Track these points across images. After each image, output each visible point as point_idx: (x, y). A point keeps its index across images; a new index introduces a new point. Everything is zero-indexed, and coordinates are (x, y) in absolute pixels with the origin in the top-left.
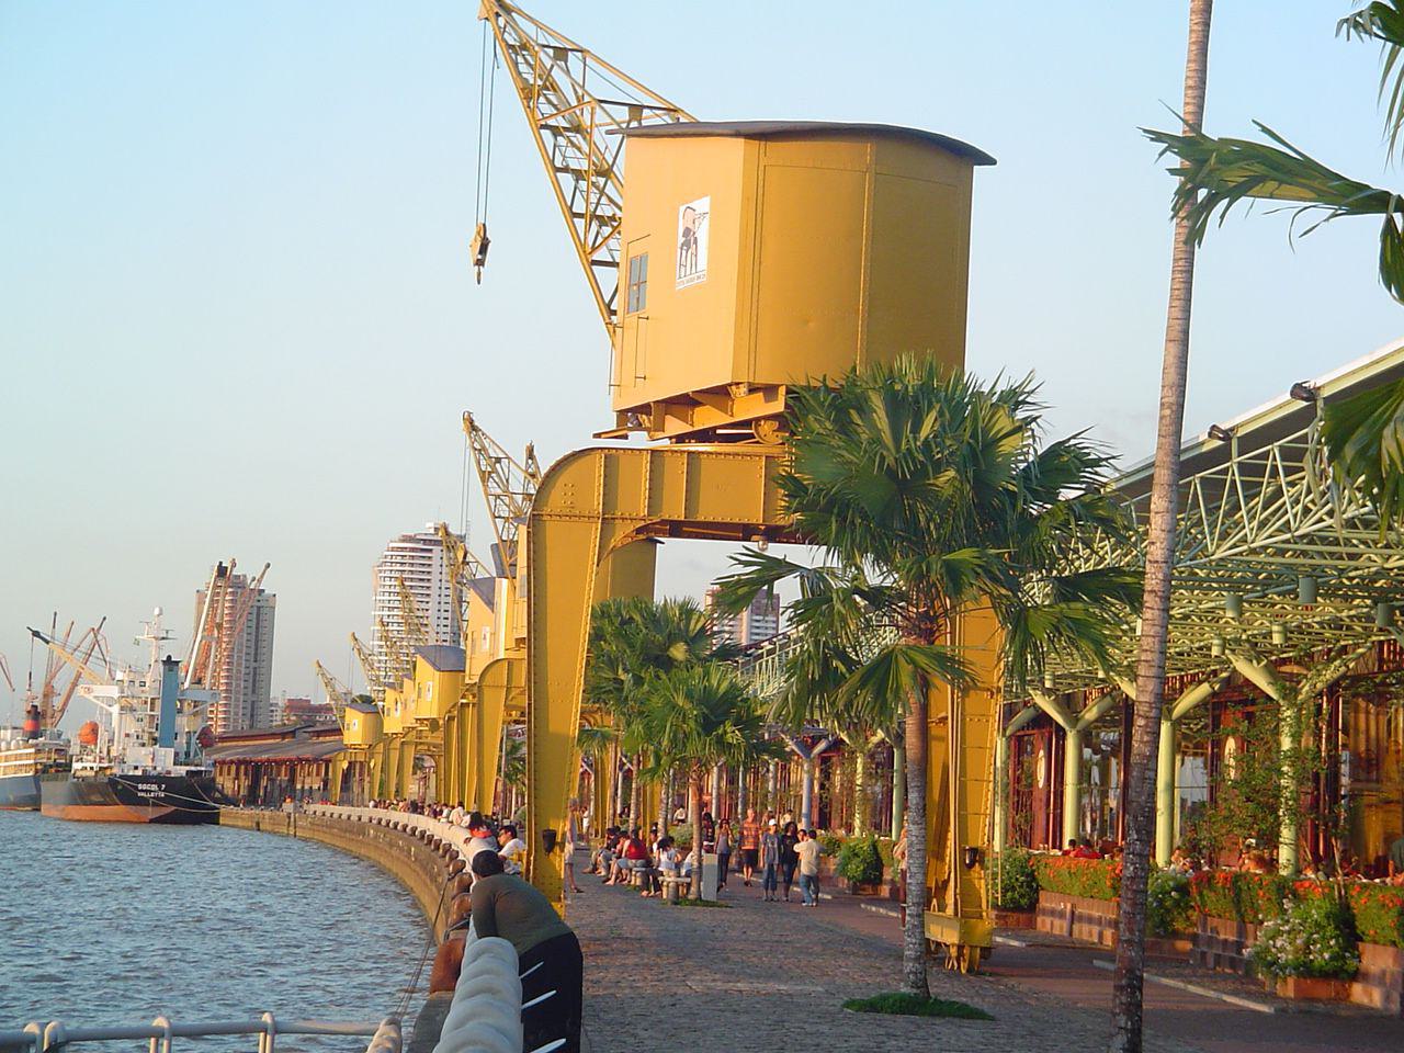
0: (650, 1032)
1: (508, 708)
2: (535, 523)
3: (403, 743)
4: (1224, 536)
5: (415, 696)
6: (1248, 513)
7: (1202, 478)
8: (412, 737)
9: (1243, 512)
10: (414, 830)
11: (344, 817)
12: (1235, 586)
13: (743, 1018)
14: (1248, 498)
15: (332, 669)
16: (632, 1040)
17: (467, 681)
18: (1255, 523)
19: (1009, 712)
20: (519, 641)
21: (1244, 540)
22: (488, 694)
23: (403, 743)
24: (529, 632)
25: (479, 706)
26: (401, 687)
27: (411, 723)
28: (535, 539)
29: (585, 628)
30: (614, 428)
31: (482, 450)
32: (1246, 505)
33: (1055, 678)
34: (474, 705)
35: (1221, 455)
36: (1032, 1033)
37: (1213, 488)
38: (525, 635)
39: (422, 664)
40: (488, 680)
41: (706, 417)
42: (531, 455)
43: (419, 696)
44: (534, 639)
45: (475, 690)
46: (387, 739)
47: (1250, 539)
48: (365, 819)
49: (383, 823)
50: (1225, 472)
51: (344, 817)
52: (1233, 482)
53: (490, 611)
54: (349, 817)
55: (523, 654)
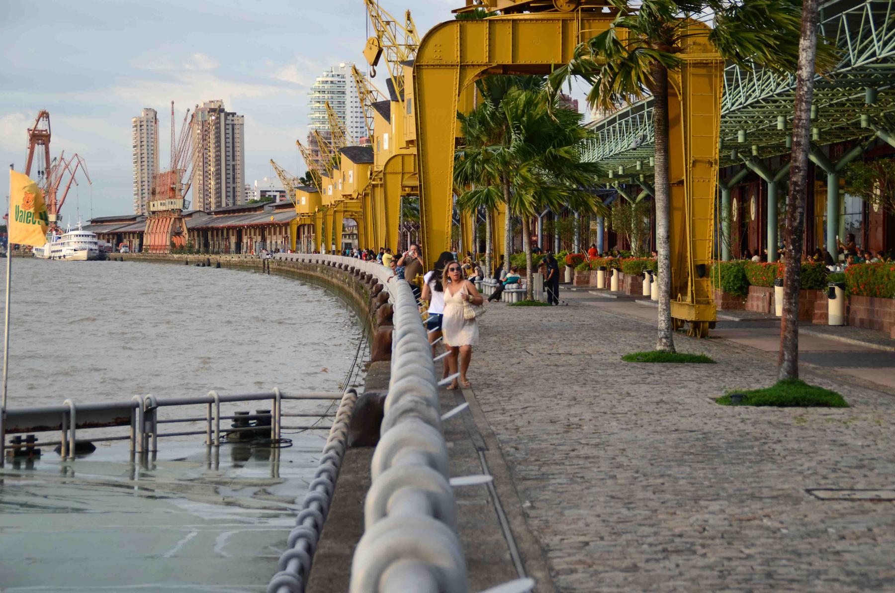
0: (506, 378)
1: (403, 187)
2: (417, 67)
3: (335, 212)
4: (861, 52)
5: (340, 181)
6: (877, 36)
7: (847, 15)
8: (341, 207)
9: (874, 36)
10: (346, 267)
11: (300, 260)
12: (873, 84)
13: (561, 369)
14: (878, 24)
15: (282, 165)
16: (495, 383)
17: (375, 169)
18: (881, 43)
19: (724, 175)
20: (411, 142)
21: (874, 54)
22: (389, 178)
23: (335, 212)
24: (417, 135)
25: (384, 186)
26: (332, 175)
27: (339, 197)
28: (417, 79)
29: (454, 129)
30: (464, 6)
31: (376, 17)
32: (876, 30)
33: (759, 149)
34: (381, 185)
36: (738, 369)
37: (854, 21)
38: (414, 137)
39: (344, 159)
40: (389, 170)
42: (409, 19)
43: (344, 180)
44: (420, 141)
45: (381, 175)
46: (323, 209)
47: (878, 52)
48: (314, 261)
49: (326, 263)
50: (862, 9)
51: (300, 260)
52: (867, 15)
53: (386, 122)
54: (303, 260)
55: (413, 150)
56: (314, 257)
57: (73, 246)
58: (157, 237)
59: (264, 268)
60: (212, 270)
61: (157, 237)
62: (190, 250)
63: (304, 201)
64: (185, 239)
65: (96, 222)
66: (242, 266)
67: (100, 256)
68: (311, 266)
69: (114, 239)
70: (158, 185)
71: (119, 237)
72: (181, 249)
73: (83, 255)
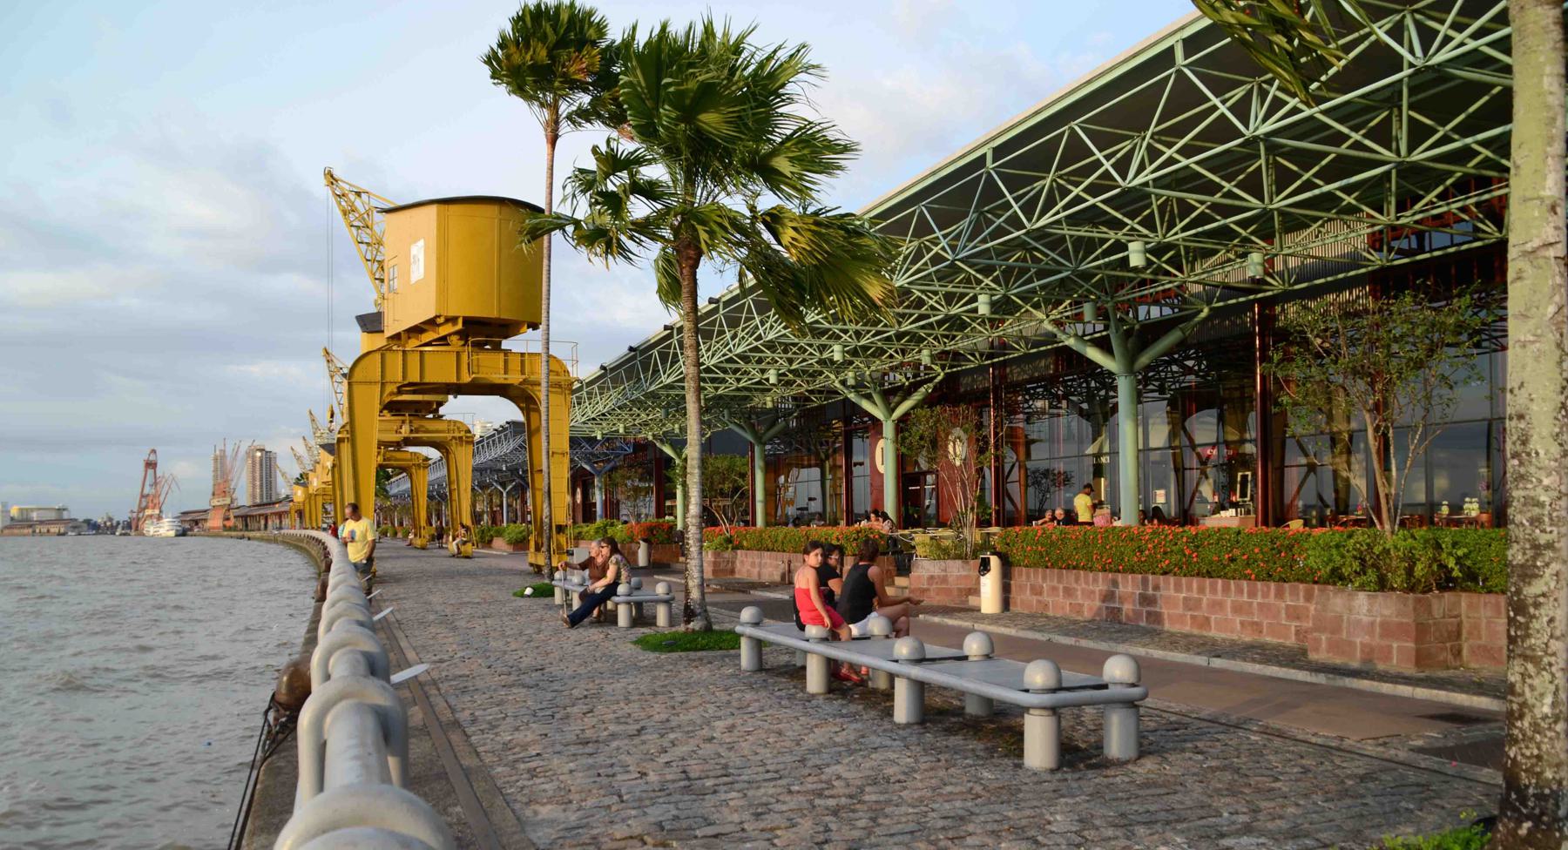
35: (669, 336)
41: (428, 336)
56: (304, 532)
57: (166, 528)
58: (215, 521)
59: (274, 541)
60: (245, 541)
61: (215, 521)
62: (235, 529)
63: (299, 494)
64: (231, 523)
65: (184, 513)
66: (261, 539)
67: (183, 533)
68: (300, 539)
69: (190, 524)
70: (222, 487)
71: (196, 522)
72: (230, 529)
73: (172, 533)
